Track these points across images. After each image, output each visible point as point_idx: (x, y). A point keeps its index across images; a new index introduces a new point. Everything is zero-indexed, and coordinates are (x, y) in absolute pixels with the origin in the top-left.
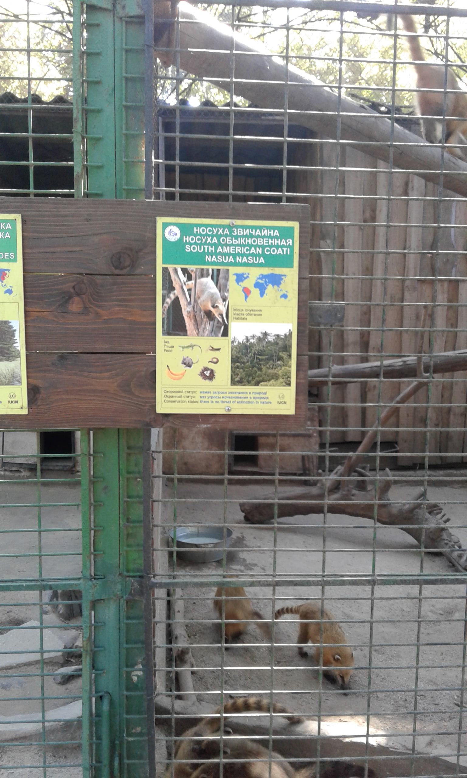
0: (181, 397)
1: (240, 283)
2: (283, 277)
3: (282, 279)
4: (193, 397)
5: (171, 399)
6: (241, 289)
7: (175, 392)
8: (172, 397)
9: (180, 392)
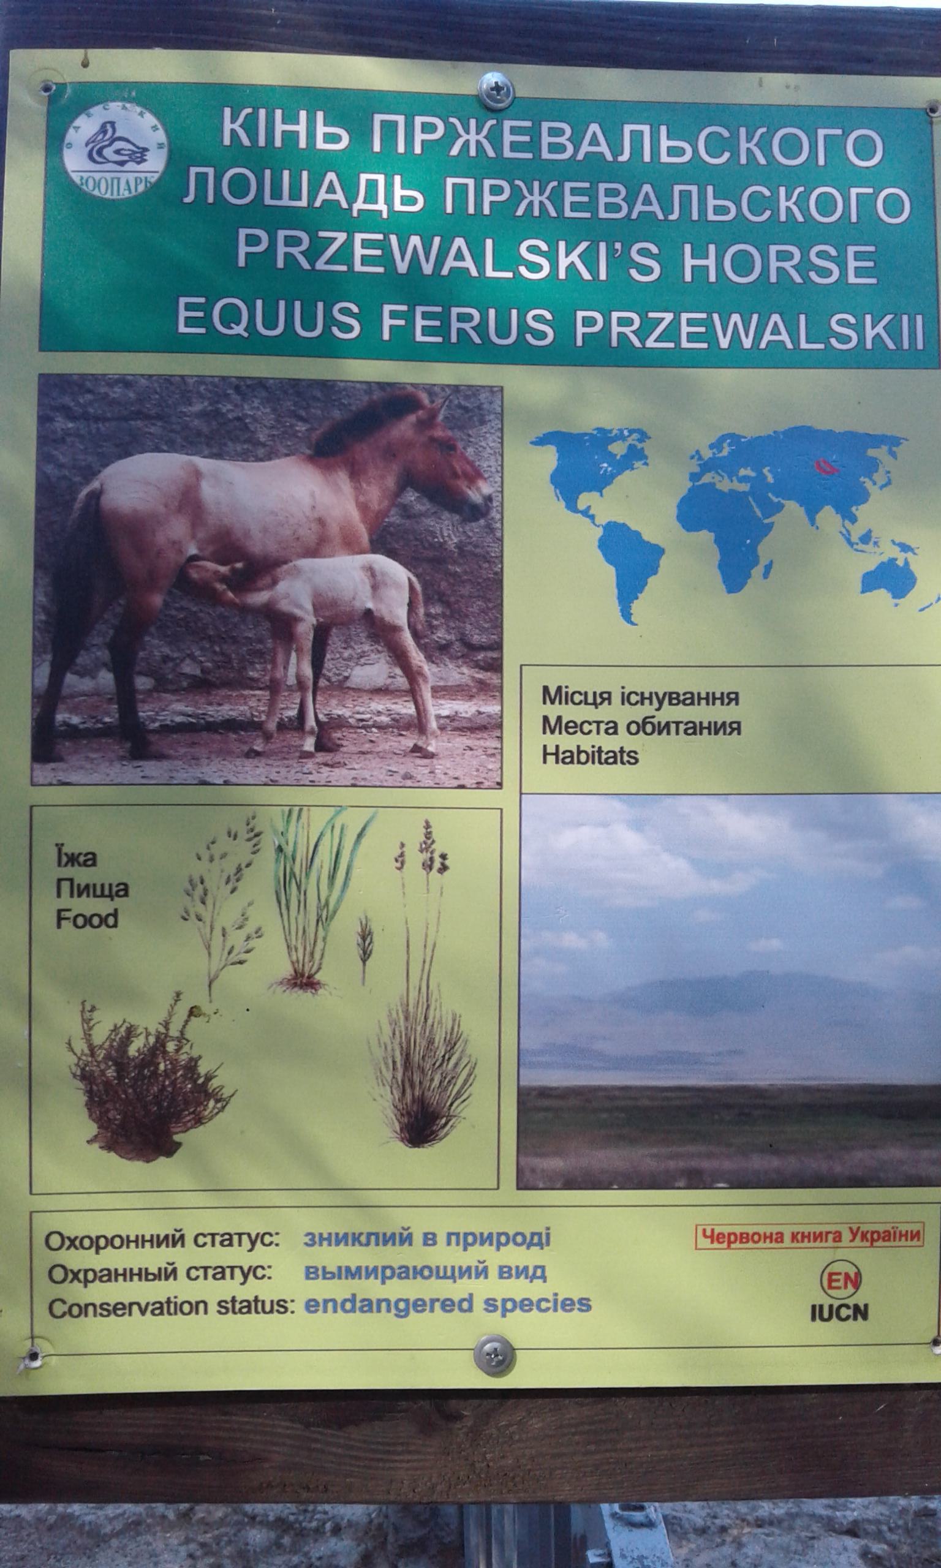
0: (169, 1273)
1: (584, 500)
2: (879, 453)
3: (872, 466)
4: (249, 1273)
5: (99, 1293)
6: (599, 532)
7: (126, 1242)
8: (110, 1275)
9: (158, 1241)
